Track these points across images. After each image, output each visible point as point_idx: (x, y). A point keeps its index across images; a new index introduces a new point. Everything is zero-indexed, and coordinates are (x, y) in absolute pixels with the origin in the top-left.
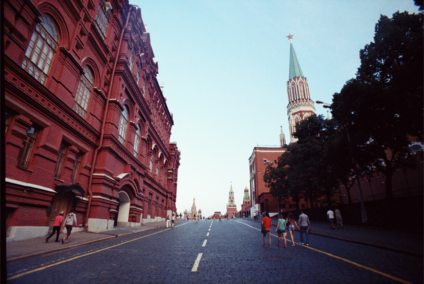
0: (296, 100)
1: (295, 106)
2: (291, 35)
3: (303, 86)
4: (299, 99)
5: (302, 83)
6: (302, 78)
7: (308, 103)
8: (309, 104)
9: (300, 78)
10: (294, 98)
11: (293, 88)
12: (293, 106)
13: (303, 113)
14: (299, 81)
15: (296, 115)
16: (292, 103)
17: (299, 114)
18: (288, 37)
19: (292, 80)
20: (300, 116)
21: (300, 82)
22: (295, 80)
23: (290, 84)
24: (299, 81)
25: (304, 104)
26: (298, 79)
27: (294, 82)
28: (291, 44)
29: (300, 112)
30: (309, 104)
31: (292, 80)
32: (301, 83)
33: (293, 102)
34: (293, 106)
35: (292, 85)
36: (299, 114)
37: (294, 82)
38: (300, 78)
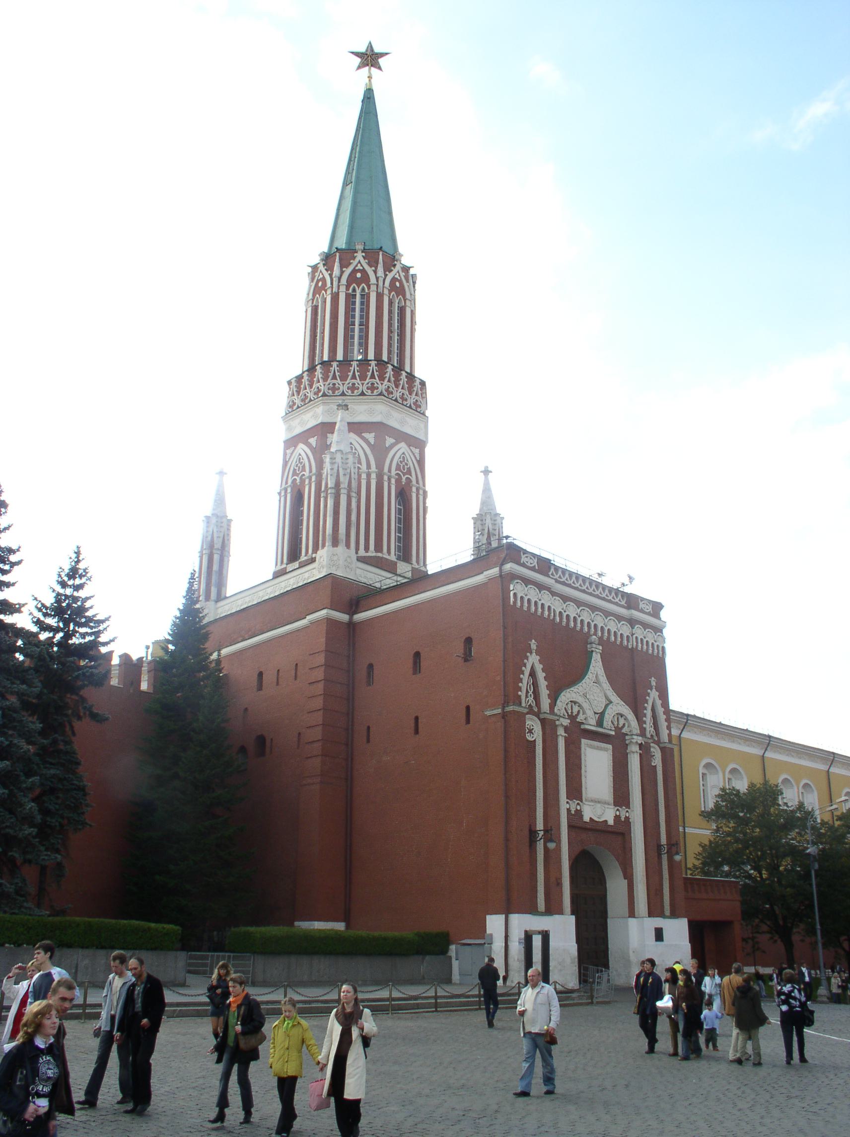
3: (402, 310)
5: (401, 291)
6: (406, 269)
11: (350, 298)
12: (343, 388)
13: (389, 441)
19: (359, 256)
22: (373, 263)
25: (397, 394)
26: (388, 269)
27: (370, 271)
28: (369, 97)
29: (379, 428)
31: (359, 256)
34: (343, 388)
35: (352, 279)
36: (370, 437)
37: (370, 271)
38: (398, 267)
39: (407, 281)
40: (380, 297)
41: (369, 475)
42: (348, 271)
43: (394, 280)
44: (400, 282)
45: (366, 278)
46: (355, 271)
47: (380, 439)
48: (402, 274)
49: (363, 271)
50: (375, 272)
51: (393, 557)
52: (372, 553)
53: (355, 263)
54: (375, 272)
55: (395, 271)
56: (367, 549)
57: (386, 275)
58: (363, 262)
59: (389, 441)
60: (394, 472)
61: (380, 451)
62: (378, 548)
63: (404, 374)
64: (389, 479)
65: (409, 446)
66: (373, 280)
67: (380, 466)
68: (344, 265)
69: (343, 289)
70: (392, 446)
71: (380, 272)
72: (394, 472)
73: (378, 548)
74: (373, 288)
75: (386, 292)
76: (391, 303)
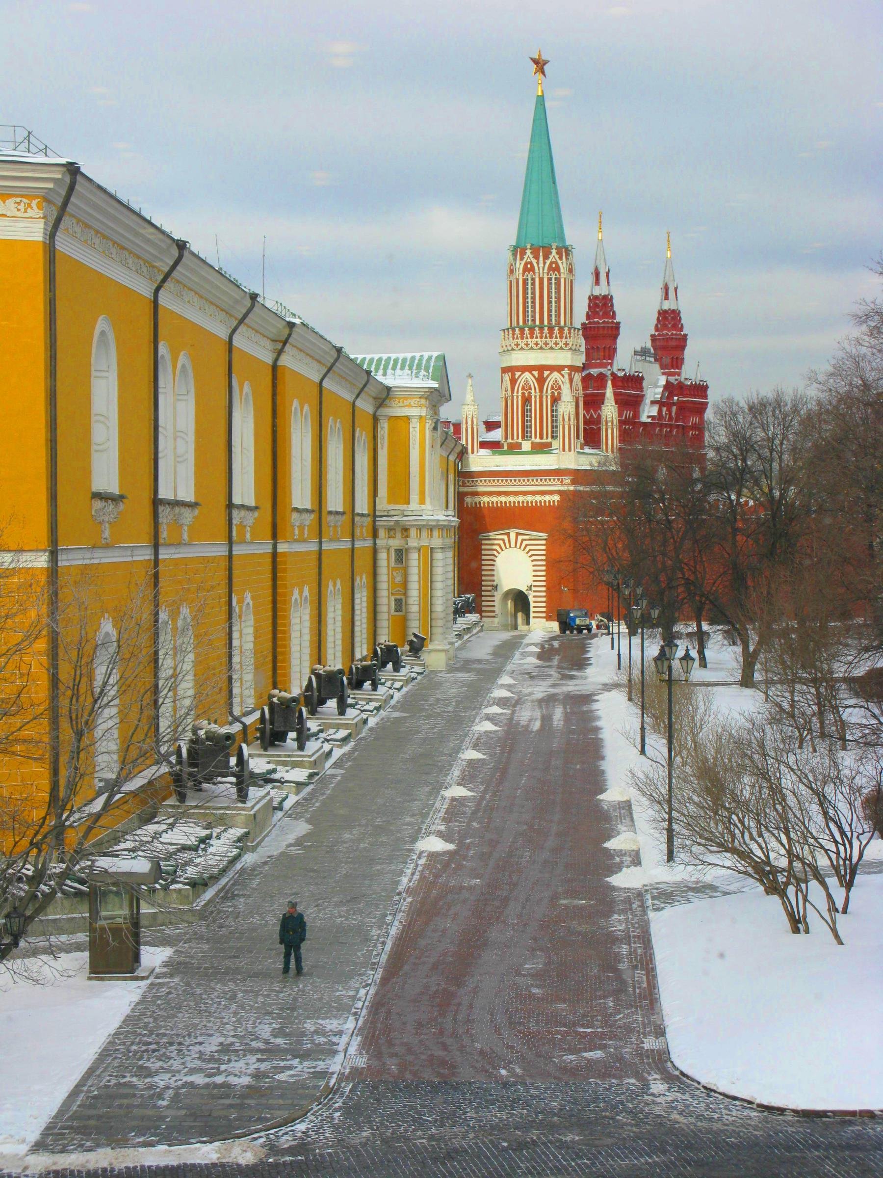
0: (532, 330)
1: (527, 345)
2: (544, 57)
3: (558, 281)
4: (541, 329)
5: (557, 269)
7: (564, 340)
8: (566, 344)
9: (554, 252)
10: (525, 321)
13: (546, 373)
14: (548, 262)
15: (527, 375)
16: (517, 331)
17: (536, 373)
18: (536, 62)
19: (528, 252)
20: (537, 380)
21: (550, 268)
22: (537, 257)
23: (520, 266)
24: (548, 262)
26: (546, 257)
27: (534, 262)
30: (566, 344)
31: (528, 252)
32: (554, 270)
33: (522, 330)
35: (525, 270)
37: (534, 262)
38: (554, 252)
39: (561, 258)
40: (541, 280)
41: (535, 397)
42: (523, 263)
43: (551, 263)
44: (556, 263)
45: (532, 269)
46: (526, 264)
47: (541, 374)
48: (557, 257)
49: (531, 263)
50: (538, 263)
51: (550, 440)
52: (538, 440)
53: (526, 257)
54: (538, 263)
55: (551, 257)
56: (536, 437)
57: (544, 263)
58: (531, 256)
59: (546, 373)
60: (549, 391)
61: (541, 381)
62: (541, 438)
63: (557, 328)
64: (547, 397)
65: (559, 372)
66: (537, 270)
67: (541, 391)
68: (522, 259)
69: (521, 276)
70: (548, 376)
71: (541, 265)
72: (549, 391)
73: (541, 438)
74: (537, 275)
75: (545, 275)
76: (550, 279)
